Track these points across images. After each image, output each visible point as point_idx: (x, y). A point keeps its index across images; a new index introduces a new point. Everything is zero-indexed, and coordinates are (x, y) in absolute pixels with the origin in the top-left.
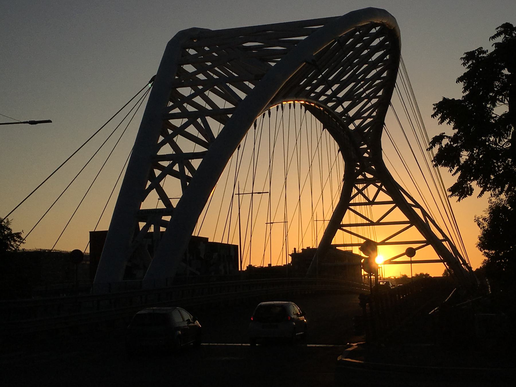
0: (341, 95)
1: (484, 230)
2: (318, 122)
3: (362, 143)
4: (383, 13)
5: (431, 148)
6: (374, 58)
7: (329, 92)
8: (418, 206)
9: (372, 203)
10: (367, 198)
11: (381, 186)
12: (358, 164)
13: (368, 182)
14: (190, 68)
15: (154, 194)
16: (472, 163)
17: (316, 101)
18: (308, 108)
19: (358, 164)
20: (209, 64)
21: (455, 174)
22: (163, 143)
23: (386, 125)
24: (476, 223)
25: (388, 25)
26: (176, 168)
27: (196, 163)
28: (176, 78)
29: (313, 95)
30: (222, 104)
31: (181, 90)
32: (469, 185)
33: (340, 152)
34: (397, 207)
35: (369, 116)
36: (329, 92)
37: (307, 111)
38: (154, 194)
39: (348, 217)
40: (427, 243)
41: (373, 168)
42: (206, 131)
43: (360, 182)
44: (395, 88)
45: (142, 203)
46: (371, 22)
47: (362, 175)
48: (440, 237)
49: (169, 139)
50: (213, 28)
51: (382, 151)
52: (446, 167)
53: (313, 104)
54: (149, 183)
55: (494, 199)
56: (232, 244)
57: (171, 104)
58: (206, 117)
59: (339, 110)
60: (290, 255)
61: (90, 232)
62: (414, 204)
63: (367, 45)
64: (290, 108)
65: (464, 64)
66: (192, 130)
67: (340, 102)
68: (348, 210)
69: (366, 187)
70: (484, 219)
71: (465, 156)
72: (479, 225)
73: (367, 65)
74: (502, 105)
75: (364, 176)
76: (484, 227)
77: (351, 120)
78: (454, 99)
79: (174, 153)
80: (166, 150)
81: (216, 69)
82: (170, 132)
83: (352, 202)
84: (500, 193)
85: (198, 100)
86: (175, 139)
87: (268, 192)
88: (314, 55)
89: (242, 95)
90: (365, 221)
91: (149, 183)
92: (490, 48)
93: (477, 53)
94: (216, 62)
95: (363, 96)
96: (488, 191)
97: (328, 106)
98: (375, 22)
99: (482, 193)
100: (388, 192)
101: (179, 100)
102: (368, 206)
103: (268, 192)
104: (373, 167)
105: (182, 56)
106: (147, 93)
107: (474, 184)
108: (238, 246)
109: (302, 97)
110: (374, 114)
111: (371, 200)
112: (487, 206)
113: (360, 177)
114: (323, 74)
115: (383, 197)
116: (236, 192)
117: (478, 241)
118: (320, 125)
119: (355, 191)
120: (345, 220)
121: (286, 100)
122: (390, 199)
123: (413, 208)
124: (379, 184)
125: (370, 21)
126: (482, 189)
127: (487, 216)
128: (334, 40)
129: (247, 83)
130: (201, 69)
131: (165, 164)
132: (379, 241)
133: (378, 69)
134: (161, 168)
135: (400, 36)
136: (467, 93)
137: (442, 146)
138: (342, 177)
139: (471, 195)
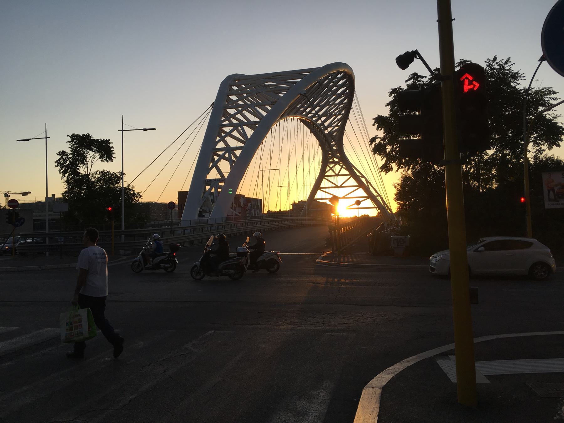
0: (320, 113)
1: (398, 190)
2: (307, 129)
4: (345, 65)
5: (371, 144)
6: (339, 92)
7: (314, 112)
8: (363, 177)
9: (337, 175)
10: (335, 172)
11: (343, 165)
12: (330, 153)
13: (335, 163)
14: (234, 98)
15: (214, 170)
16: (392, 153)
17: (306, 117)
18: (301, 121)
19: (330, 153)
20: (245, 95)
22: (219, 141)
24: (393, 187)
26: (227, 155)
27: (238, 153)
30: (253, 119)
31: (229, 111)
32: (390, 166)
33: (320, 146)
34: (352, 178)
36: (314, 112)
38: (214, 170)
39: (324, 183)
40: (368, 198)
42: (244, 134)
43: (331, 163)
46: (338, 71)
47: (332, 159)
48: (375, 194)
49: (223, 139)
50: (247, 74)
53: (304, 118)
55: (404, 173)
56: (259, 198)
57: (223, 118)
58: (244, 126)
59: (319, 122)
60: (291, 205)
61: (178, 192)
65: (390, 96)
66: (235, 133)
67: (320, 117)
69: (334, 166)
70: (398, 184)
71: (389, 148)
73: (335, 96)
75: (333, 160)
76: (398, 189)
77: (326, 128)
78: (383, 116)
79: (225, 147)
80: (221, 145)
81: (249, 98)
82: (223, 135)
84: (408, 170)
85: (239, 116)
86: (226, 139)
89: (264, 114)
90: (334, 186)
91: (211, 164)
94: (249, 94)
96: (401, 168)
98: (340, 71)
99: (398, 169)
102: (335, 177)
104: (338, 155)
105: (229, 91)
107: (394, 165)
108: (262, 200)
110: (339, 124)
111: (337, 173)
113: (331, 160)
115: (344, 171)
116: (261, 169)
117: (394, 196)
118: (308, 130)
119: (328, 168)
120: (322, 185)
121: (289, 116)
122: (348, 173)
123: (360, 178)
126: (397, 167)
127: (400, 182)
129: (267, 106)
131: (221, 153)
132: (341, 197)
133: (342, 99)
136: (391, 113)
137: (376, 143)
138: (321, 161)
139: (392, 170)
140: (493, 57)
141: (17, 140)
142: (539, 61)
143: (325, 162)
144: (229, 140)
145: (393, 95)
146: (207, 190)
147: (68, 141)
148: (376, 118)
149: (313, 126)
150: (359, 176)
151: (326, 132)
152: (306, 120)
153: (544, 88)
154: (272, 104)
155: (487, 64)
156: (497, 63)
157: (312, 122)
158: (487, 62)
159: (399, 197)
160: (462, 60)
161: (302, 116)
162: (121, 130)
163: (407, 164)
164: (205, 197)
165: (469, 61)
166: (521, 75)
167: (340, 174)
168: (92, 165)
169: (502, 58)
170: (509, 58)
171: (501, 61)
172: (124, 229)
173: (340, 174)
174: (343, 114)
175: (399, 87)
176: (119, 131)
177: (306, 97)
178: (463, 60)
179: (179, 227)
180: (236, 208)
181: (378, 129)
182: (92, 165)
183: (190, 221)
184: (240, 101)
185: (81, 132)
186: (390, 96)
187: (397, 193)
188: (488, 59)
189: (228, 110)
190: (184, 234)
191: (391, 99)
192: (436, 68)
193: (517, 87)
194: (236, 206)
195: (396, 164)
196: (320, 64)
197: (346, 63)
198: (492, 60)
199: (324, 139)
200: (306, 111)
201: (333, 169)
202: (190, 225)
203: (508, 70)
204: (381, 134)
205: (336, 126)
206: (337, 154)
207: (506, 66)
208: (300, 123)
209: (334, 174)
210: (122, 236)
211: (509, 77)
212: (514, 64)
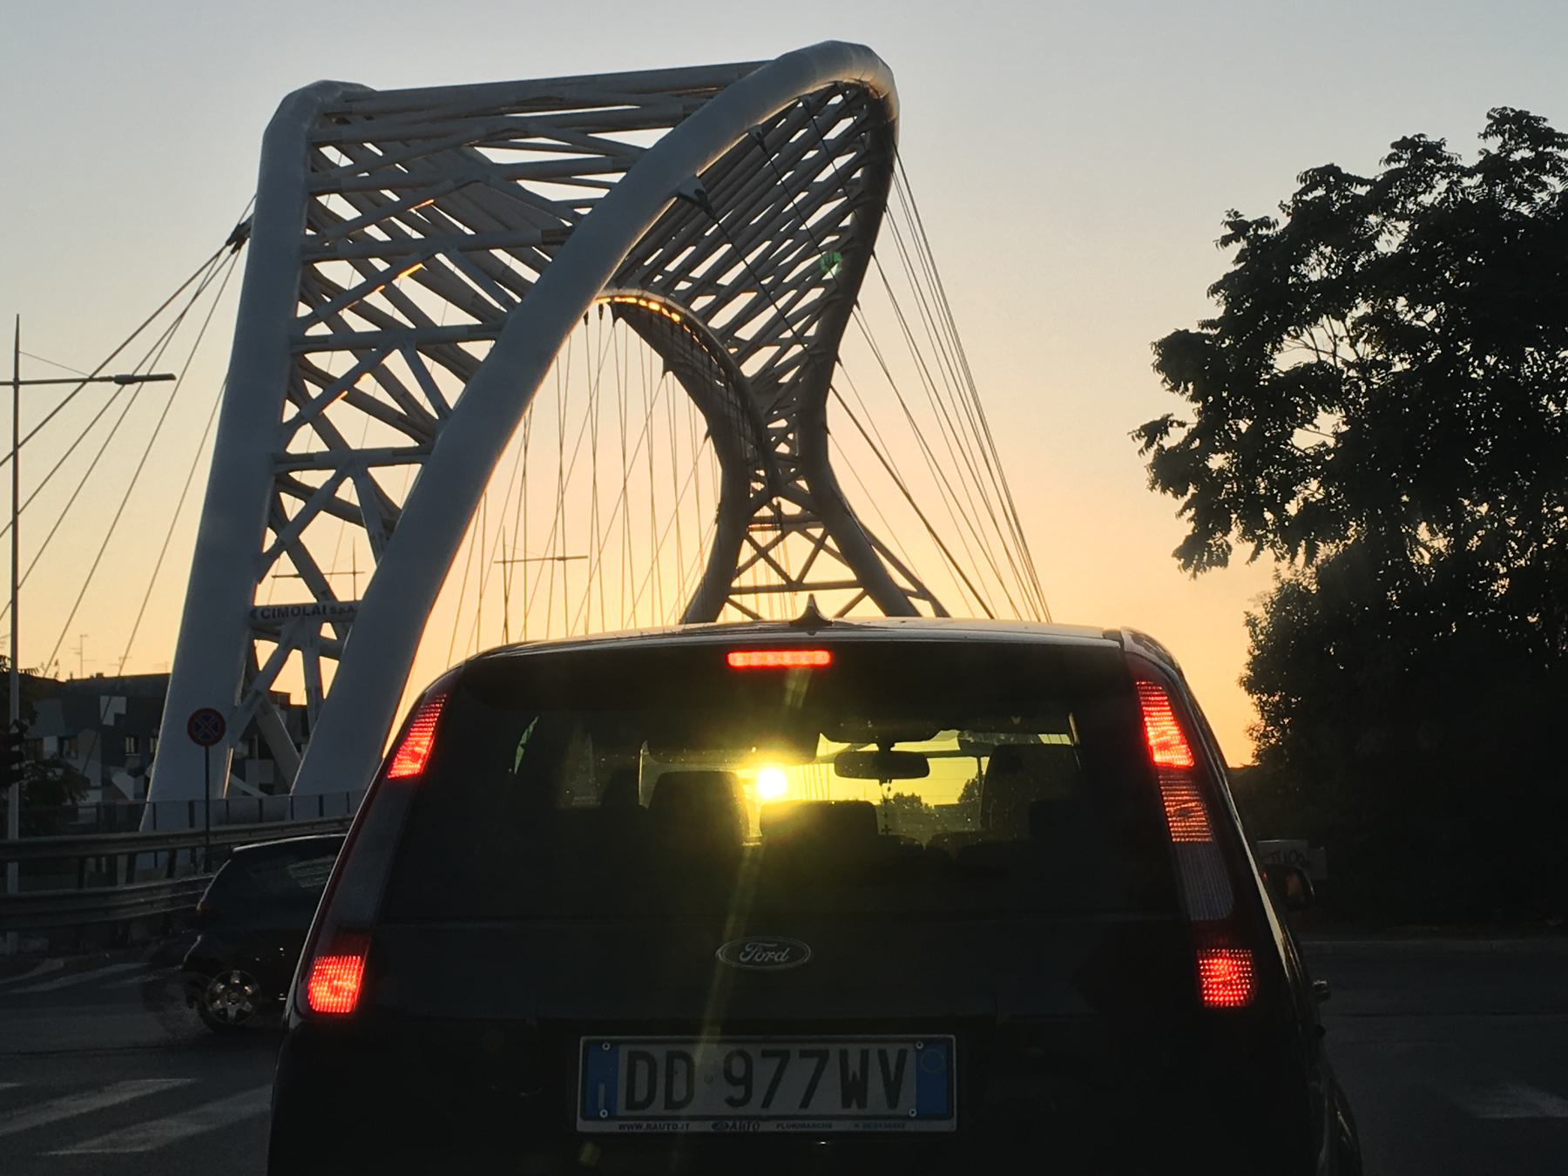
0: (726, 280)
3: (775, 412)
4: (864, 53)
6: (821, 178)
8: (924, 594)
11: (824, 537)
12: (762, 473)
13: (783, 524)
14: (339, 206)
15: (284, 563)
17: (666, 295)
18: (620, 311)
23: (843, 362)
24: (1247, 630)
25: (872, 87)
26: (348, 492)
28: (309, 236)
29: (683, 285)
33: (710, 439)
34: (867, 598)
35: (798, 338)
37: (621, 321)
38: (284, 563)
41: (802, 488)
44: (872, 257)
45: (259, 587)
46: (836, 82)
47: (772, 507)
49: (313, 414)
50: (379, 85)
51: (829, 436)
57: (304, 310)
59: (719, 321)
63: (814, 140)
64: (601, 318)
67: (726, 296)
68: (727, 605)
69: (781, 538)
74: (1295, 348)
75: (777, 509)
78: (1187, 331)
80: (306, 441)
82: (314, 391)
86: (328, 412)
87: (586, 557)
88: (698, 175)
93: (1254, 226)
94: (411, 190)
95: (786, 280)
97: (692, 311)
98: (845, 81)
101: (328, 300)
102: (787, 594)
103: (586, 557)
104: (803, 484)
105: (313, 170)
106: (210, 276)
109: (632, 286)
110: (811, 332)
111: (794, 577)
112: (1272, 587)
113: (765, 512)
114: (716, 226)
115: (831, 568)
119: (746, 553)
122: (849, 574)
123: (913, 600)
124: (817, 532)
125: (832, 80)
128: (747, 134)
129: (499, 254)
130: (375, 211)
131: (315, 479)
135: (898, 118)
138: (713, 513)
144: (339, 413)
145: (1236, 248)
146: (261, 668)
149: (689, 337)
150: (906, 593)
151: (751, 367)
152: (665, 312)
154: (547, 240)
157: (686, 320)
160: (1509, 111)
161: (647, 294)
164: (258, 694)
167: (806, 581)
172: (20, 836)
173: (806, 581)
174: (828, 281)
175: (1262, 219)
177: (708, 210)
178: (1512, 110)
180: (248, 763)
183: (321, 798)
184: (679, 282)
189: (320, 266)
191: (1226, 261)
192: (1404, 138)
194: (246, 752)
196: (767, 48)
197: (868, 45)
199: (736, 405)
200: (691, 275)
201: (772, 553)
202: (321, 814)
204: (1185, 410)
206: (796, 477)
208: (615, 320)
209: (777, 580)
210: (10, 864)
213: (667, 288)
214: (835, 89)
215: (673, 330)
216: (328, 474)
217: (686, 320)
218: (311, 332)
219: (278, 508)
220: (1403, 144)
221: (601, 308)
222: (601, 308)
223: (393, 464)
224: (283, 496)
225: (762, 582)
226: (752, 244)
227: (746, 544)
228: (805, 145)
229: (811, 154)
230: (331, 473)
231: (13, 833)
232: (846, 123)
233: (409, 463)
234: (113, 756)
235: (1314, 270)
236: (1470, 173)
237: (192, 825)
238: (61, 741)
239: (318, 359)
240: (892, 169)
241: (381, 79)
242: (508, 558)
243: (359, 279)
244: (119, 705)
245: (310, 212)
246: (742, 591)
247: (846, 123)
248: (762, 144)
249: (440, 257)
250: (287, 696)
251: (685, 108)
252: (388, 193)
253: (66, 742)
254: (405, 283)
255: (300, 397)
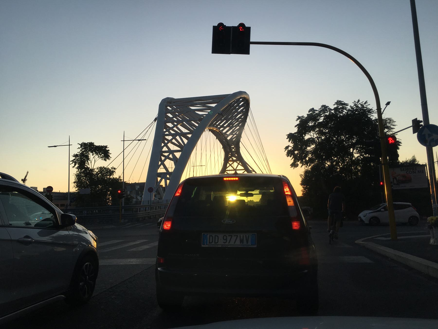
0: (225, 126)
4: (245, 93)
6: (239, 111)
8: (254, 171)
11: (239, 163)
13: (233, 161)
15: (162, 166)
17: (216, 128)
18: (210, 130)
19: (230, 153)
21: (292, 159)
24: (300, 176)
26: (171, 156)
27: (178, 155)
29: (219, 126)
33: (223, 149)
37: (210, 132)
45: (158, 170)
47: (232, 158)
49: (166, 145)
52: (291, 157)
54: (160, 163)
55: (306, 168)
57: (165, 130)
59: (224, 132)
62: (252, 170)
65: (297, 120)
67: (225, 128)
72: (301, 177)
78: (292, 133)
80: (165, 149)
82: (166, 142)
83: (226, 169)
92: (306, 116)
99: (302, 166)
100: (242, 166)
104: (236, 155)
107: (299, 163)
109: (212, 127)
110: (237, 133)
111: (235, 168)
112: (304, 170)
113: (231, 159)
115: (240, 167)
119: (228, 165)
122: (243, 168)
123: (252, 172)
124: (238, 162)
126: (302, 165)
127: (303, 174)
129: (193, 122)
130: (175, 116)
131: (166, 154)
134: (164, 156)
139: (298, 166)
140: (358, 100)
141: (48, 147)
142: (386, 105)
143: (226, 160)
144: (170, 145)
145: (299, 120)
147: (79, 148)
148: (288, 135)
151: (229, 138)
152: (216, 130)
153: (387, 118)
155: (354, 104)
156: (360, 104)
157: (219, 131)
158: (354, 103)
159: (304, 183)
161: (214, 128)
162: (123, 140)
163: (306, 163)
164: (158, 185)
165: (342, 102)
166: (374, 111)
167: (237, 169)
168: (95, 163)
169: (362, 101)
170: (367, 101)
171: (362, 102)
172: (124, 205)
173: (237, 169)
176: (121, 141)
178: (339, 100)
179: (141, 205)
180: (156, 195)
181: (289, 141)
182: (95, 163)
185: (87, 141)
186: (297, 120)
187: (302, 180)
188: (354, 101)
189: (167, 124)
190: (156, 210)
191: (298, 122)
193: (371, 118)
194: (156, 194)
195: (301, 162)
198: (357, 101)
201: (232, 165)
203: (366, 107)
204: (292, 145)
205: (236, 134)
206: (235, 154)
207: (365, 105)
209: (232, 169)
211: (367, 111)
212: (370, 104)
213: (217, 127)
214: (241, 98)
215: (217, 133)
216: (168, 154)
217: (219, 131)
218: (166, 133)
219: (161, 158)
220: (323, 106)
221: (207, 130)
222: (207, 130)
223: (177, 152)
224: (162, 157)
225: (230, 169)
226: (229, 120)
227: (228, 164)
228: (237, 106)
229: (237, 107)
230: (169, 153)
231: (123, 205)
232: (242, 103)
233: (180, 152)
234: (137, 194)
235: (311, 124)
236: (332, 110)
237: (148, 204)
238: (130, 192)
239: (167, 137)
240: (249, 110)
241: (176, 97)
242: (194, 166)
243: (172, 126)
244: (138, 187)
245: (166, 116)
246: (227, 170)
247: (242, 103)
248: (230, 106)
249: (184, 122)
250: (162, 185)
251: (219, 101)
252: (177, 113)
253: (131, 192)
254: (179, 126)
255: (164, 143)
